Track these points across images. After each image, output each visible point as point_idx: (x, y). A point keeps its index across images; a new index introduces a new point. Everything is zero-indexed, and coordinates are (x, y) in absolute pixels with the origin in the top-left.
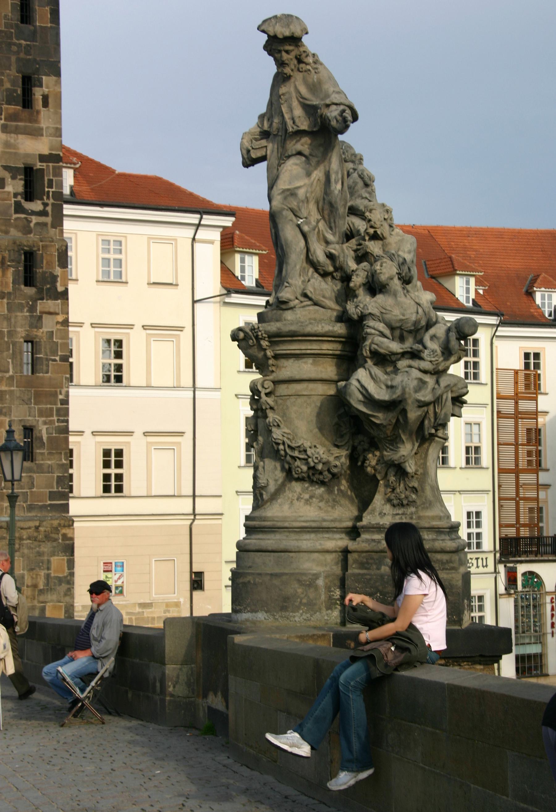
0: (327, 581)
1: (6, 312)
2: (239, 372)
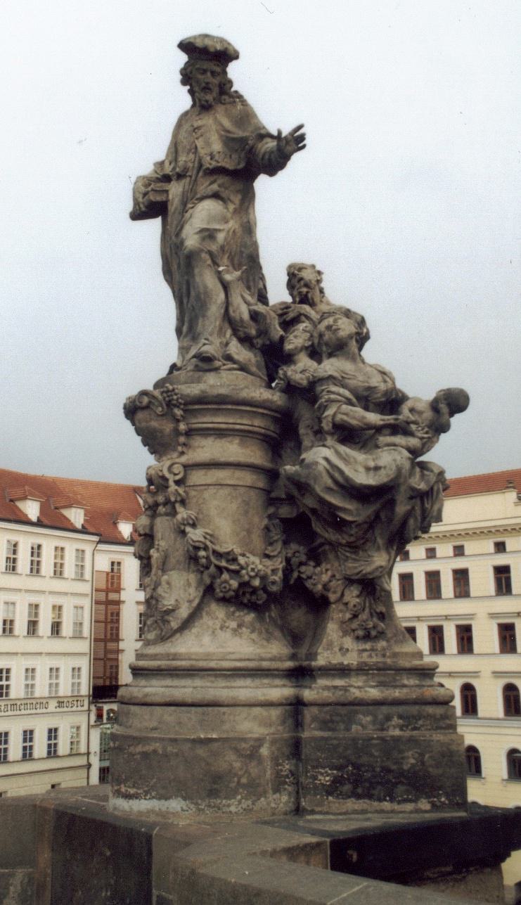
0: (273, 748)
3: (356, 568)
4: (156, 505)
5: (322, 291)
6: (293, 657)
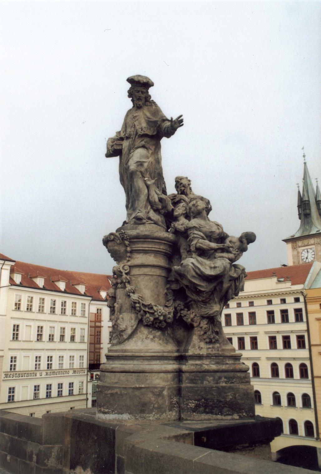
0: (169, 392)
3: (205, 311)
4: (117, 283)
5: (190, 189)
6: (178, 351)
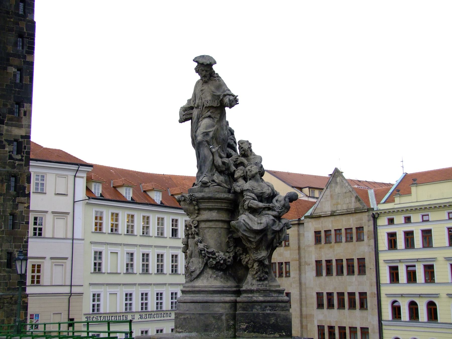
0: (226, 317)
1: (2, 202)
2: (92, 232)
3: (256, 256)
5: (251, 151)
